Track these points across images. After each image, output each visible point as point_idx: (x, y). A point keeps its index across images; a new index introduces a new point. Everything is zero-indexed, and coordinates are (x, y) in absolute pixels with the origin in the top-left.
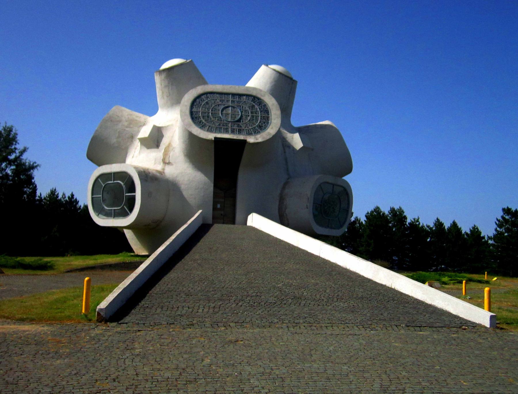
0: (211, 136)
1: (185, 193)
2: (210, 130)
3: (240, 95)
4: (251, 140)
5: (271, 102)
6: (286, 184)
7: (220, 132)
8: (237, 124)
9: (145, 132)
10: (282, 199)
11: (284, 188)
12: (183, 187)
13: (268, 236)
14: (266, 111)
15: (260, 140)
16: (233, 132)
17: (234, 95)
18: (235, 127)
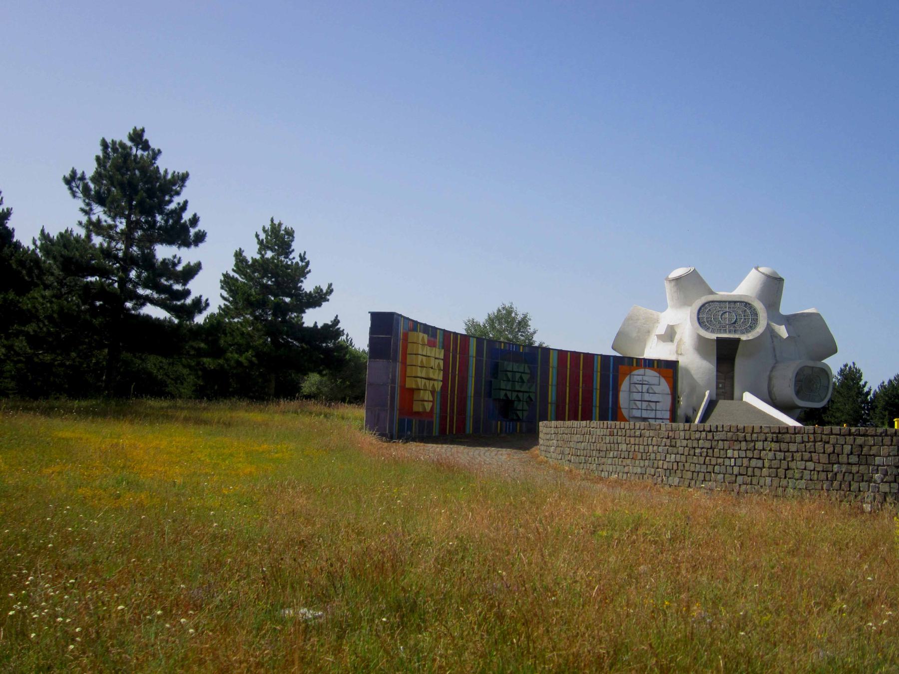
0: (714, 336)
1: (695, 377)
2: (713, 332)
3: (735, 302)
4: (744, 338)
5: (759, 306)
6: (774, 367)
7: (719, 331)
8: (733, 326)
9: (661, 329)
10: (770, 379)
11: (771, 371)
12: (693, 372)
13: (755, 408)
14: (755, 314)
15: (751, 338)
16: (730, 332)
17: (730, 302)
18: (732, 328)
